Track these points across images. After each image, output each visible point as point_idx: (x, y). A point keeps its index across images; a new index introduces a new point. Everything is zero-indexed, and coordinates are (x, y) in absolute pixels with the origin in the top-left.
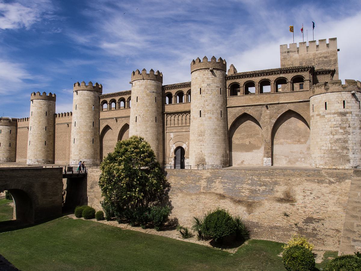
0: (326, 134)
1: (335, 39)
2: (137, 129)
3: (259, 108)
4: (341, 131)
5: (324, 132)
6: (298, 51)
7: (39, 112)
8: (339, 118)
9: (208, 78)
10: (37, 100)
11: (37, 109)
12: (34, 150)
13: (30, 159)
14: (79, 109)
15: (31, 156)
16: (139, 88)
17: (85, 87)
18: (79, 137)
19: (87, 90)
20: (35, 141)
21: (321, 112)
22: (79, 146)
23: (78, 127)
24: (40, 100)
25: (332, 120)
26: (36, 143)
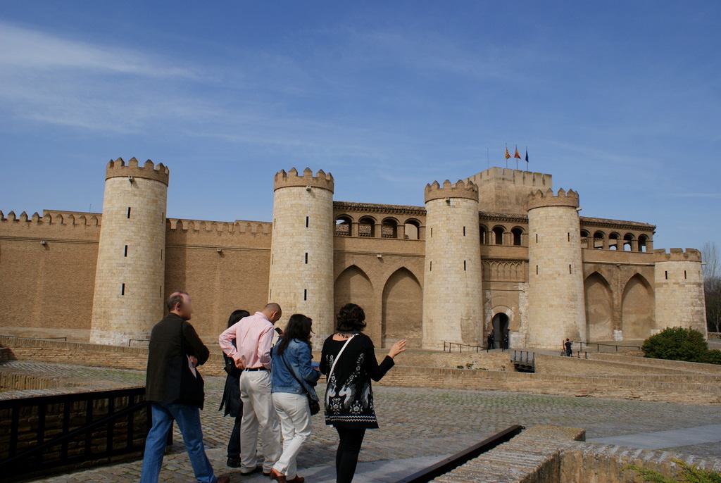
0: (687, 305)
1: (550, 176)
2: (469, 282)
3: (610, 267)
4: (699, 302)
5: (685, 302)
6: (514, 181)
7: (152, 212)
8: (697, 289)
9: (576, 222)
10: (146, 181)
11: (147, 205)
12: (139, 307)
13: (128, 330)
14: (315, 226)
15: (128, 323)
16: (466, 213)
17: (326, 183)
18: (317, 288)
19: (328, 190)
20: (142, 286)
21: (680, 281)
22: (319, 306)
23: (315, 266)
24: (152, 182)
25: (693, 290)
26: (144, 290)
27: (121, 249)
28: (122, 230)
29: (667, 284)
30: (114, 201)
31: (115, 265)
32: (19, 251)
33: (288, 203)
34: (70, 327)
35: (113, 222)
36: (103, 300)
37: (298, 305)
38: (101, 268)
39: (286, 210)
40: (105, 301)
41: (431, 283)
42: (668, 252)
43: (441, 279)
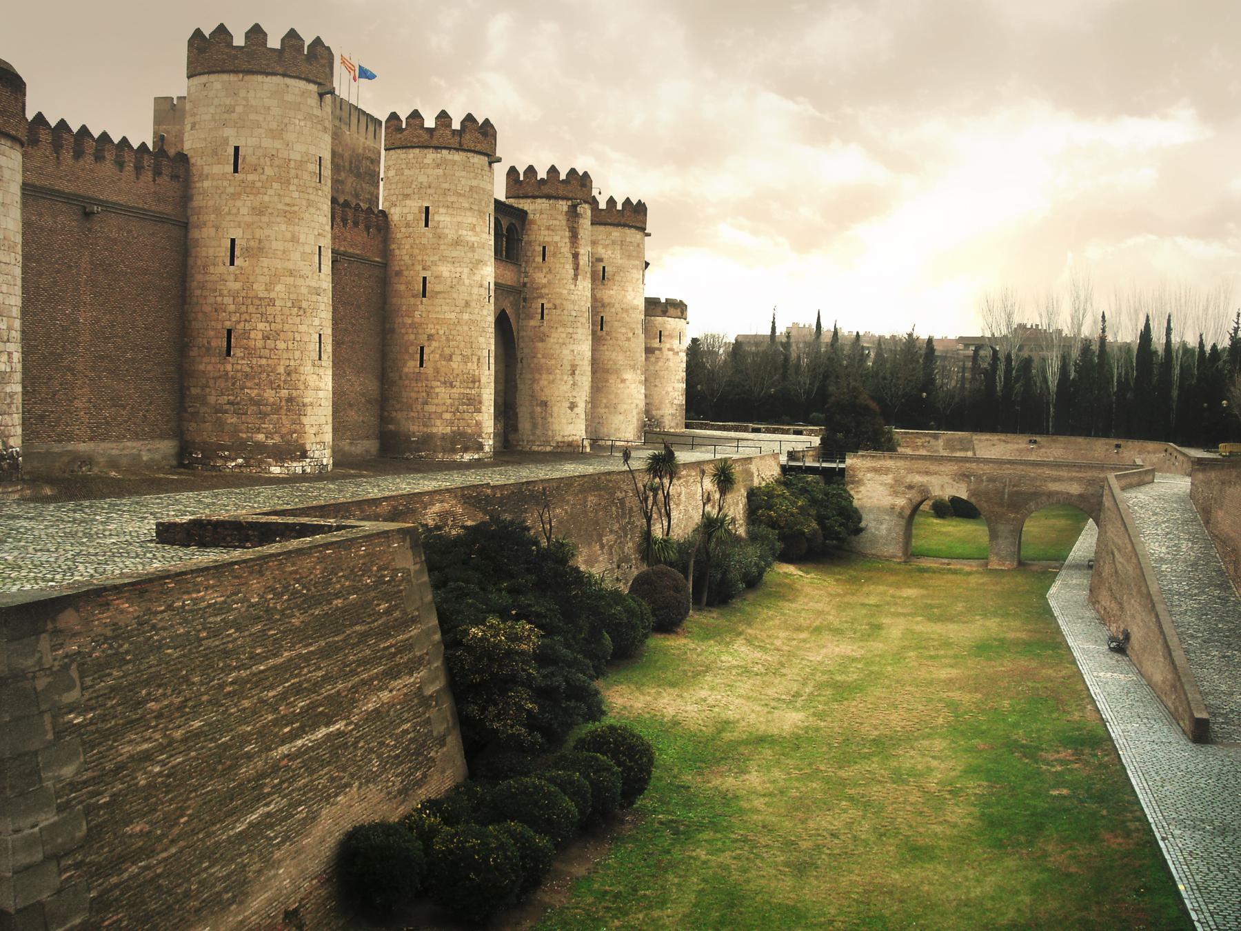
27: (313, 253)
28: (312, 210)
29: (660, 349)
30: (291, 136)
31: (304, 290)
32: (42, 229)
33: (463, 181)
34: (137, 437)
35: (292, 188)
36: (281, 370)
37: (484, 380)
38: (261, 295)
39: (460, 195)
40: (289, 374)
41: (543, 341)
42: (663, 301)
43: (564, 335)
